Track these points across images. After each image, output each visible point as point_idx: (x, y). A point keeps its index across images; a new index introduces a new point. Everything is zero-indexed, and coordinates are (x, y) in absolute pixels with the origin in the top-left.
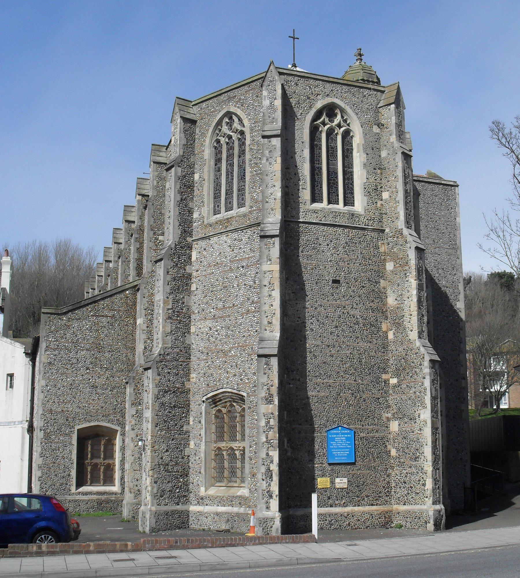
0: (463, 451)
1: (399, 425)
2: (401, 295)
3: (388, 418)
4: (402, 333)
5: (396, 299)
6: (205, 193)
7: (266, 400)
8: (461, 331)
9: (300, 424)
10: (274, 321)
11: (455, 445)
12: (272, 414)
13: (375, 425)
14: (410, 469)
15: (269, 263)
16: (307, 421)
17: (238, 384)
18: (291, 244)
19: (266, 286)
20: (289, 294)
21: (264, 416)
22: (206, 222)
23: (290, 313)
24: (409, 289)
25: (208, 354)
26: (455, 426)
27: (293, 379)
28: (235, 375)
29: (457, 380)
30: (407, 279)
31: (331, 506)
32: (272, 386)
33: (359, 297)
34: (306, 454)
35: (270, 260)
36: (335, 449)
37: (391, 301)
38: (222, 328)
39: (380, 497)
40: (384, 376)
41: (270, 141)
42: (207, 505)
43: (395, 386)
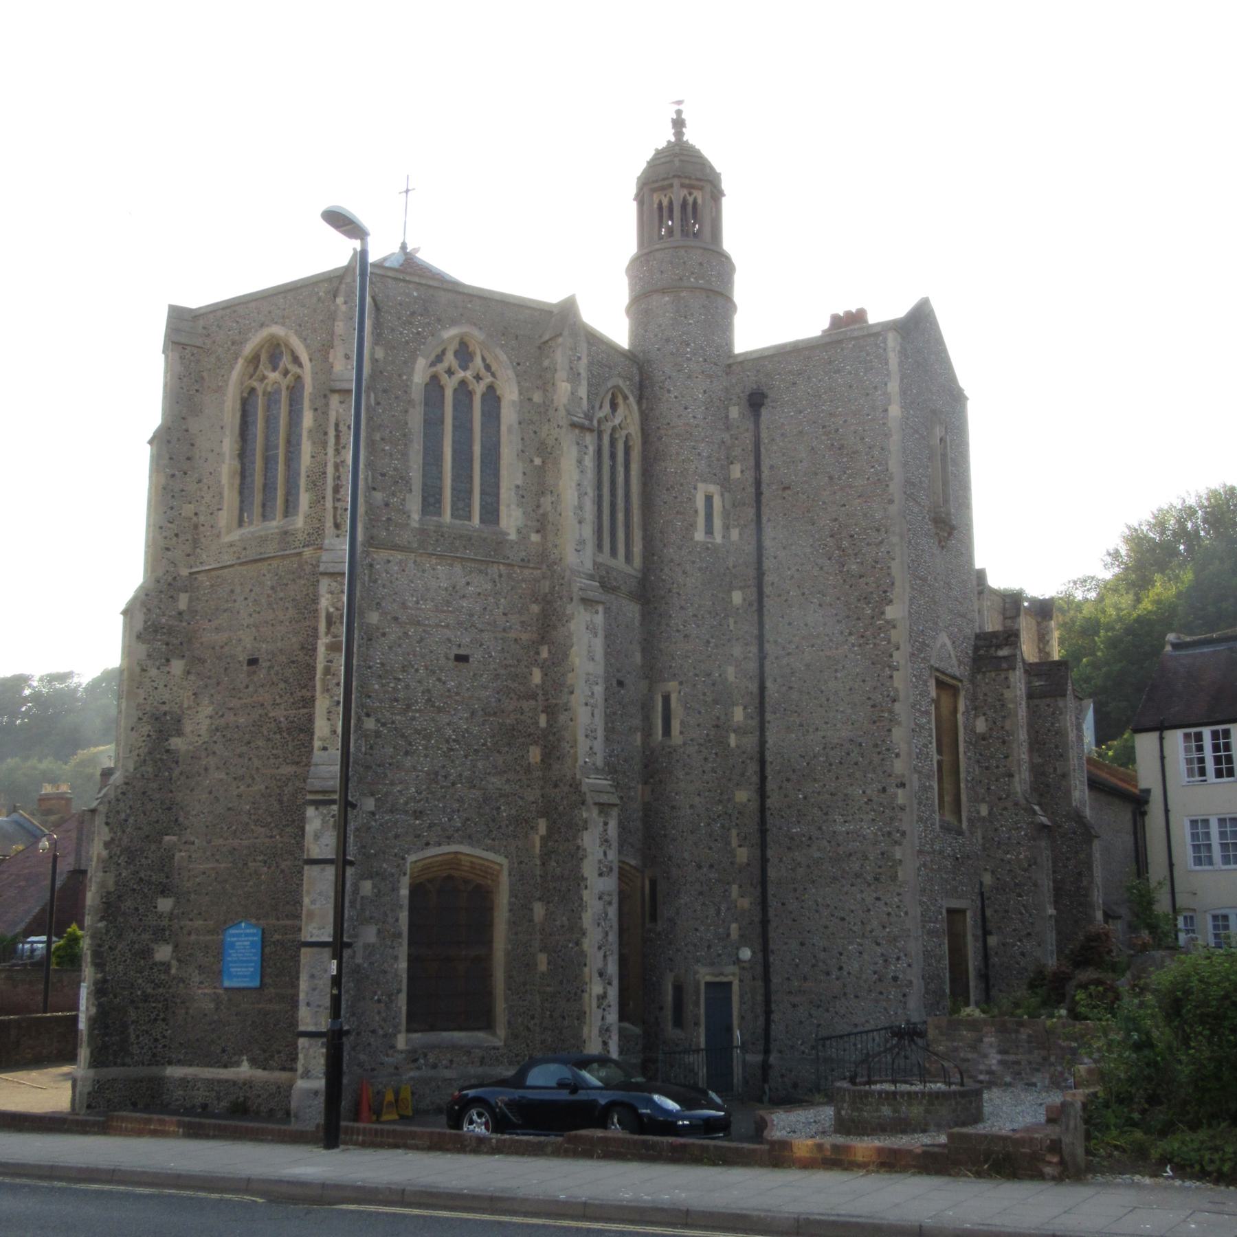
0: (898, 959)
8: (895, 674)
11: (878, 944)
16: (200, 914)
20: (188, 698)
26: (878, 899)
27: (185, 843)
29: (884, 790)
31: (225, 1066)
33: (285, 682)
36: (235, 962)
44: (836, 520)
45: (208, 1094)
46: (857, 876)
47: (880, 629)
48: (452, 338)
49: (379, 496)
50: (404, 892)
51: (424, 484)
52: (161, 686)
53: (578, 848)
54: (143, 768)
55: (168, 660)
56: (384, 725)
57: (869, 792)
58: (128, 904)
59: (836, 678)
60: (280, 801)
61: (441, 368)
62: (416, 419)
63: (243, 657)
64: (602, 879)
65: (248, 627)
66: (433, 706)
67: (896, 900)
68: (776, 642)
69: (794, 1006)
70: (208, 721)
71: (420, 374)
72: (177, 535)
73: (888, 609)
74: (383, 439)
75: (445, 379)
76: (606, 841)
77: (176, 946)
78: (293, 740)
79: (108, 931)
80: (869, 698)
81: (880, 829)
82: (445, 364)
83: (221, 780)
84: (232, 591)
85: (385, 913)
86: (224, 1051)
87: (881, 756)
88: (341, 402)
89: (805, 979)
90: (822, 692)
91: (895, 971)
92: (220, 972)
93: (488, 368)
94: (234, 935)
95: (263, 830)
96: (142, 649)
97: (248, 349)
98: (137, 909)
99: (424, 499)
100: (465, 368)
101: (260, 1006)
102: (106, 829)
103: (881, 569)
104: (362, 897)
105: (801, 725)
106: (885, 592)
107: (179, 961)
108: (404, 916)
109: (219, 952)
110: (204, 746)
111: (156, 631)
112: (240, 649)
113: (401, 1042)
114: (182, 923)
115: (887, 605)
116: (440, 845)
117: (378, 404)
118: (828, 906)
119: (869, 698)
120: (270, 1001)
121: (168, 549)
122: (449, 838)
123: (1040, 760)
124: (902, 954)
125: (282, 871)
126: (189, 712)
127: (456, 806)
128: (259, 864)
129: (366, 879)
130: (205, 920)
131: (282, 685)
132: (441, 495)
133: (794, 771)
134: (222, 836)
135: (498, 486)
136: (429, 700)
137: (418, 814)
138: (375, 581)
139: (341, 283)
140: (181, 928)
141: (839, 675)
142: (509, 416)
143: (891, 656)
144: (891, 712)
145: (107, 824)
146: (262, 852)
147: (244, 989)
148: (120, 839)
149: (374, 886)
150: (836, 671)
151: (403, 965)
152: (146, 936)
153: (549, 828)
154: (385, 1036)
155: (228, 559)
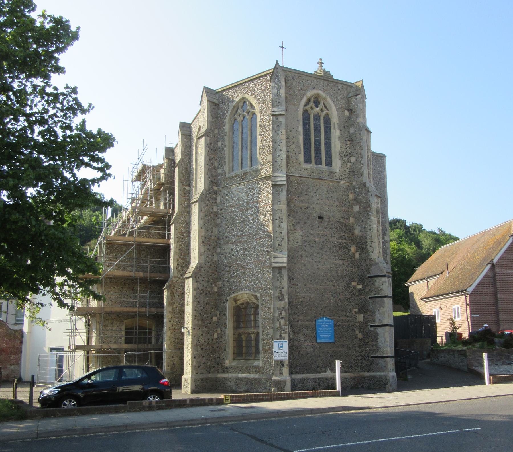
1: (364, 317)
2: (365, 228)
3: (355, 312)
4: (365, 254)
5: (361, 231)
6: (226, 155)
7: (279, 298)
10: (283, 244)
12: (283, 308)
13: (347, 316)
14: (372, 347)
15: (279, 203)
16: (303, 313)
17: (253, 288)
18: (291, 191)
19: (277, 219)
20: (290, 226)
21: (278, 309)
22: (227, 176)
23: (291, 239)
24: (371, 224)
25: (230, 267)
27: (293, 285)
28: (251, 282)
30: (369, 217)
31: (320, 373)
32: (283, 288)
34: (303, 336)
35: (280, 202)
36: (321, 332)
37: (357, 232)
38: (241, 249)
39: (351, 366)
40: (353, 284)
41: (277, 119)
42: (230, 373)
43: (360, 290)
45: (313, 384)
60: (337, 273)
65: (317, 204)
70: (301, 237)
78: (341, 251)
83: (309, 262)
84: (308, 188)
86: (318, 367)
92: (315, 337)
94: (321, 322)
95: (330, 283)
101: (334, 349)
107: (294, 332)
109: (315, 329)
110: (300, 247)
112: (314, 212)
114: (295, 317)
120: (338, 347)
125: (340, 299)
126: (291, 232)
128: (329, 296)
130: (306, 316)
131: (334, 229)
134: (311, 284)
146: (330, 291)
147: (325, 343)
155: (305, 174)
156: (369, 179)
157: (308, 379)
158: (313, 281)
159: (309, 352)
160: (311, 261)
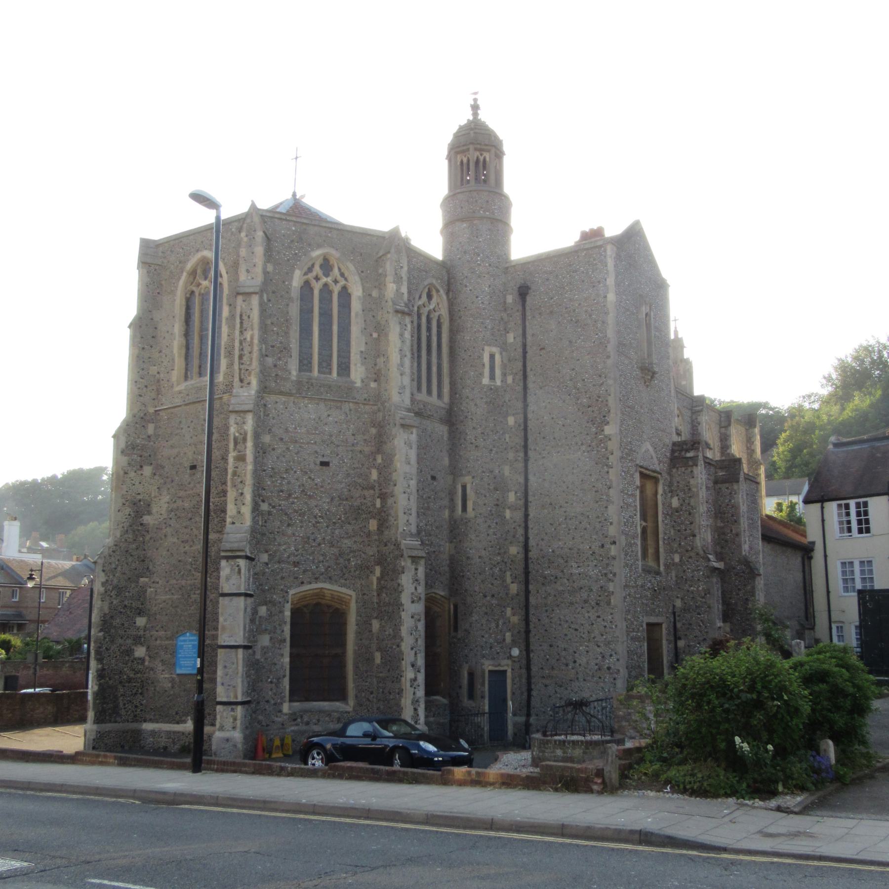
0: (611, 655)
8: (610, 470)
9: (157, 631)
11: (599, 646)
26: (599, 617)
27: (153, 582)
29: (603, 546)
36: (181, 657)
44: (573, 369)
46: (586, 601)
47: (601, 440)
48: (318, 257)
49: (270, 361)
50: (288, 614)
51: (300, 352)
52: (137, 483)
53: (399, 585)
54: (126, 536)
55: (141, 467)
56: (274, 507)
57: (593, 547)
58: (117, 622)
59: (573, 473)
61: (311, 276)
62: (294, 310)
63: (187, 464)
64: (413, 605)
65: (190, 445)
66: (306, 495)
67: (610, 617)
68: (535, 450)
69: (546, 686)
70: (166, 505)
71: (297, 280)
72: (146, 386)
73: (606, 428)
74: (272, 323)
75: (314, 283)
76: (417, 580)
77: (148, 648)
79: (105, 638)
80: (594, 487)
81: (600, 572)
82: (314, 274)
83: (174, 543)
84: (180, 422)
85: (275, 627)
86: (177, 713)
87: (601, 524)
88: (244, 301)
89: (553, 668)
90: (564, 482)
91: (609, 664)
92: (174, 665)
93: (342, 275)
96: (125, 460)
97: (189, 266)
98: (123, 625)
99: (300, 361)
100: (327, 275)
102: (103, 574)
103: (602, 402)
104: (260, 617)
105: (551, 504)
106: (604, 417)
107: (150, 657)
108: (287, 629)
111: (133, 448)
112: (185, 459)
113: (286, 708)
114: (152, 633)
115: (606, 425)
116: (310, 583)
117: (269, 301)
118: (567, 621)
119: (594, 487)
121: (140, 396)
122: (316, 579)
123: (722, 524)
124: (613, 653)
127: (321, 558)
129: (263, 605)
132: (311, 359)
133: (546, 534)
135: (349, 352)
136: (303, 491)
137: (296, 564)
138: (268, 415)
139: (243, 223)
140: (151, 636)
141: (575, 471)
142: (356, 306)
143: (608, 459)
144: (608, 495)
145: (103, 571)
148: (112, 581)
149: (268, 610)
150: (573, 468)
151: (287, 660)
152: (129, 641)
153: (382, 573)
154: (275, 704)
155: (178, 401)
156: (241, 381)
157: (160, 732)
158: (177, 573)
159: (167, 689)
160: (177, 541)
